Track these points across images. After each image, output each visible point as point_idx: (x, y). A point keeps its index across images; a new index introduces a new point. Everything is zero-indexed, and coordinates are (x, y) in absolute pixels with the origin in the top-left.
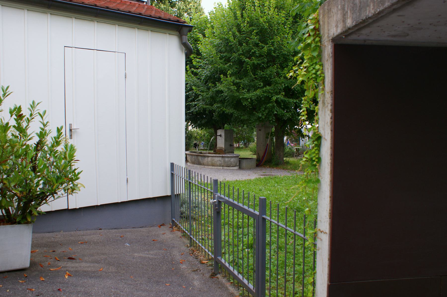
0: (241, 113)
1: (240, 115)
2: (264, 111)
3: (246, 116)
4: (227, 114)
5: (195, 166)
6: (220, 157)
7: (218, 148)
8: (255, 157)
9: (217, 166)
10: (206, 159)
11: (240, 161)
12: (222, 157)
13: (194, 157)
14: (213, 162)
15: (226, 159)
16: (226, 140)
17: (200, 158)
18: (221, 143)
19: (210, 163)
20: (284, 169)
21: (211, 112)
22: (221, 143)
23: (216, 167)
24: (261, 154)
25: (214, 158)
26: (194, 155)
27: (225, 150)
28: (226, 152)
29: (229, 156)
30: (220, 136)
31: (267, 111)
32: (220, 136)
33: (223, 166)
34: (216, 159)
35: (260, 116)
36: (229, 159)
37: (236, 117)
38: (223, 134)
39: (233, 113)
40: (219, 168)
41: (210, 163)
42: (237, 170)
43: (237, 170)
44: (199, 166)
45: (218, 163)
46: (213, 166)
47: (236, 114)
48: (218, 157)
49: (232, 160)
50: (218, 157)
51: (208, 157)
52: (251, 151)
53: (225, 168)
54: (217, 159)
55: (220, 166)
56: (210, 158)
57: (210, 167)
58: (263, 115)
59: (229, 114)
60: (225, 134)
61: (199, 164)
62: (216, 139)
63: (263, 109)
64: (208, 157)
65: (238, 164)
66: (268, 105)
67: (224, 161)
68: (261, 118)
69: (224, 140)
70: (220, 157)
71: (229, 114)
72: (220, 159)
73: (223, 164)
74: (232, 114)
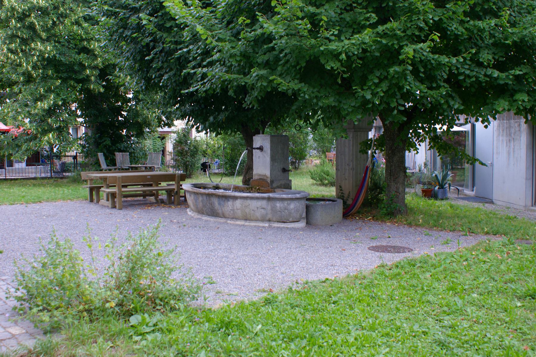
0: (318, 92)
1: (316, 97)
2: (377, 85)
3: (331, 99)
4: (284, 94)
5: (205, 218)
6: (263, 198)
7: (255, 177)
8: (331, 192)
9: (257, 220)
10: (230, 203)
11: (307, 207)
12: (269, 199)
13: (201, 198)
14: (247, 210)
15: (278, 205)
16: (273, 159)
17: (216, 202)
18: (262, 166)
19: (239, 213)
20: (410, 225)
21: (243, 90)
22: (262, 166)
23: (253, 224)
24: (349, 187)
25: (249, 202)
26: (202, 194)
27: (272, 182)
28: (275, 185)
29: (284, 196)
30: (261, 149)
31: (384, 86)
32: (261, 149)
33: (269, 221)
34: (254, 204)
35: (369, 96)
36: (286, 203)
37: (305, 101)
38: (267, 146)
39: (299, 90)
40: (261, 224)
41: (239, 213)
42: (302, 229)
43: (302, 229)
44: (212, 219)
45: (258, 214)
46: (246, 220)
47: (307, 92)
48: (257, 198)
49: (292, 206)
50: (257, 198)
51: (235, 198)
52: (312, 178)
53: (276, 225)
54: (256, 204)
55: (263, 220)
56: (238, 203)
57: (239, 222)
58: (374, 94)
59: (290, 92)
60: (272, 142)
61: (214, 213)
62: (250, 156)
63: (376, 81)
64: (235, 198)
65: (304, 215)
66: (391, 70)
67: (273, 209)
68: (368, 102)
69: (268, 159)
70: (263, 198)
71: (290, 92)
72: (264, 203)
73: (269, 216)
74: (296, 94)
